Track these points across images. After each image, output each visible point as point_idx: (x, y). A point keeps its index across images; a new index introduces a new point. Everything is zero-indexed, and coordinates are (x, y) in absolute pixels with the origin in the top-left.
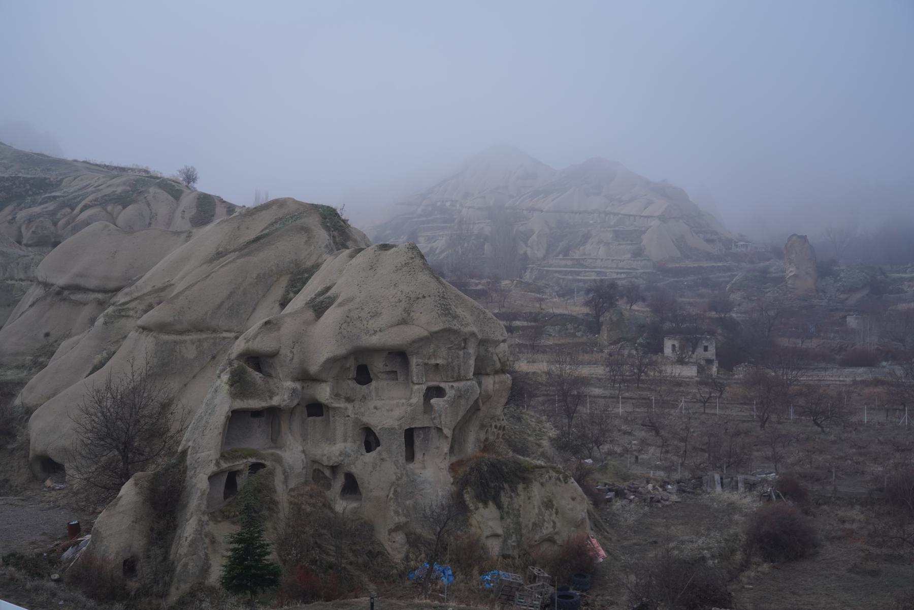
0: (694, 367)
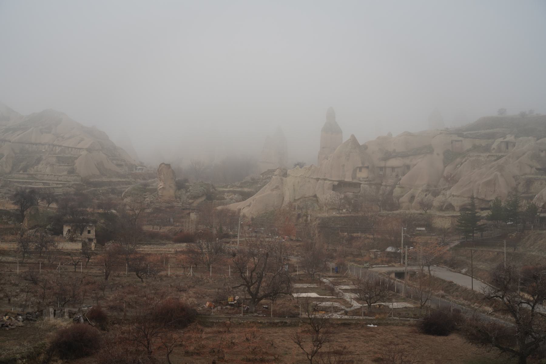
0: (80, 243)
